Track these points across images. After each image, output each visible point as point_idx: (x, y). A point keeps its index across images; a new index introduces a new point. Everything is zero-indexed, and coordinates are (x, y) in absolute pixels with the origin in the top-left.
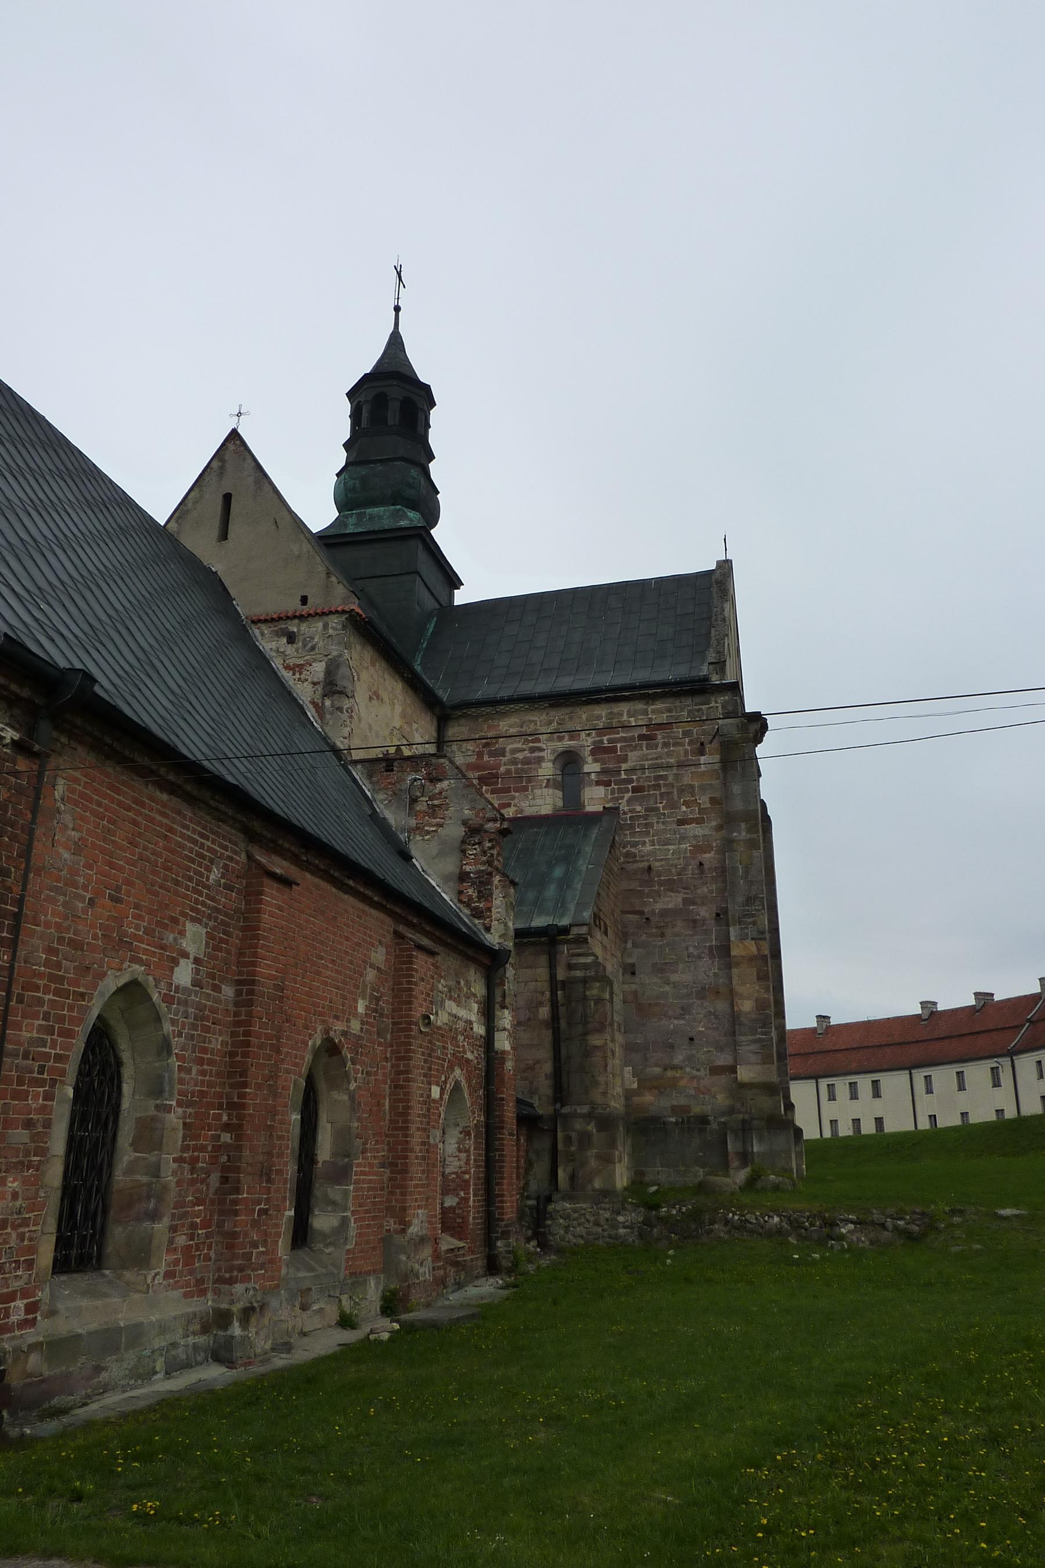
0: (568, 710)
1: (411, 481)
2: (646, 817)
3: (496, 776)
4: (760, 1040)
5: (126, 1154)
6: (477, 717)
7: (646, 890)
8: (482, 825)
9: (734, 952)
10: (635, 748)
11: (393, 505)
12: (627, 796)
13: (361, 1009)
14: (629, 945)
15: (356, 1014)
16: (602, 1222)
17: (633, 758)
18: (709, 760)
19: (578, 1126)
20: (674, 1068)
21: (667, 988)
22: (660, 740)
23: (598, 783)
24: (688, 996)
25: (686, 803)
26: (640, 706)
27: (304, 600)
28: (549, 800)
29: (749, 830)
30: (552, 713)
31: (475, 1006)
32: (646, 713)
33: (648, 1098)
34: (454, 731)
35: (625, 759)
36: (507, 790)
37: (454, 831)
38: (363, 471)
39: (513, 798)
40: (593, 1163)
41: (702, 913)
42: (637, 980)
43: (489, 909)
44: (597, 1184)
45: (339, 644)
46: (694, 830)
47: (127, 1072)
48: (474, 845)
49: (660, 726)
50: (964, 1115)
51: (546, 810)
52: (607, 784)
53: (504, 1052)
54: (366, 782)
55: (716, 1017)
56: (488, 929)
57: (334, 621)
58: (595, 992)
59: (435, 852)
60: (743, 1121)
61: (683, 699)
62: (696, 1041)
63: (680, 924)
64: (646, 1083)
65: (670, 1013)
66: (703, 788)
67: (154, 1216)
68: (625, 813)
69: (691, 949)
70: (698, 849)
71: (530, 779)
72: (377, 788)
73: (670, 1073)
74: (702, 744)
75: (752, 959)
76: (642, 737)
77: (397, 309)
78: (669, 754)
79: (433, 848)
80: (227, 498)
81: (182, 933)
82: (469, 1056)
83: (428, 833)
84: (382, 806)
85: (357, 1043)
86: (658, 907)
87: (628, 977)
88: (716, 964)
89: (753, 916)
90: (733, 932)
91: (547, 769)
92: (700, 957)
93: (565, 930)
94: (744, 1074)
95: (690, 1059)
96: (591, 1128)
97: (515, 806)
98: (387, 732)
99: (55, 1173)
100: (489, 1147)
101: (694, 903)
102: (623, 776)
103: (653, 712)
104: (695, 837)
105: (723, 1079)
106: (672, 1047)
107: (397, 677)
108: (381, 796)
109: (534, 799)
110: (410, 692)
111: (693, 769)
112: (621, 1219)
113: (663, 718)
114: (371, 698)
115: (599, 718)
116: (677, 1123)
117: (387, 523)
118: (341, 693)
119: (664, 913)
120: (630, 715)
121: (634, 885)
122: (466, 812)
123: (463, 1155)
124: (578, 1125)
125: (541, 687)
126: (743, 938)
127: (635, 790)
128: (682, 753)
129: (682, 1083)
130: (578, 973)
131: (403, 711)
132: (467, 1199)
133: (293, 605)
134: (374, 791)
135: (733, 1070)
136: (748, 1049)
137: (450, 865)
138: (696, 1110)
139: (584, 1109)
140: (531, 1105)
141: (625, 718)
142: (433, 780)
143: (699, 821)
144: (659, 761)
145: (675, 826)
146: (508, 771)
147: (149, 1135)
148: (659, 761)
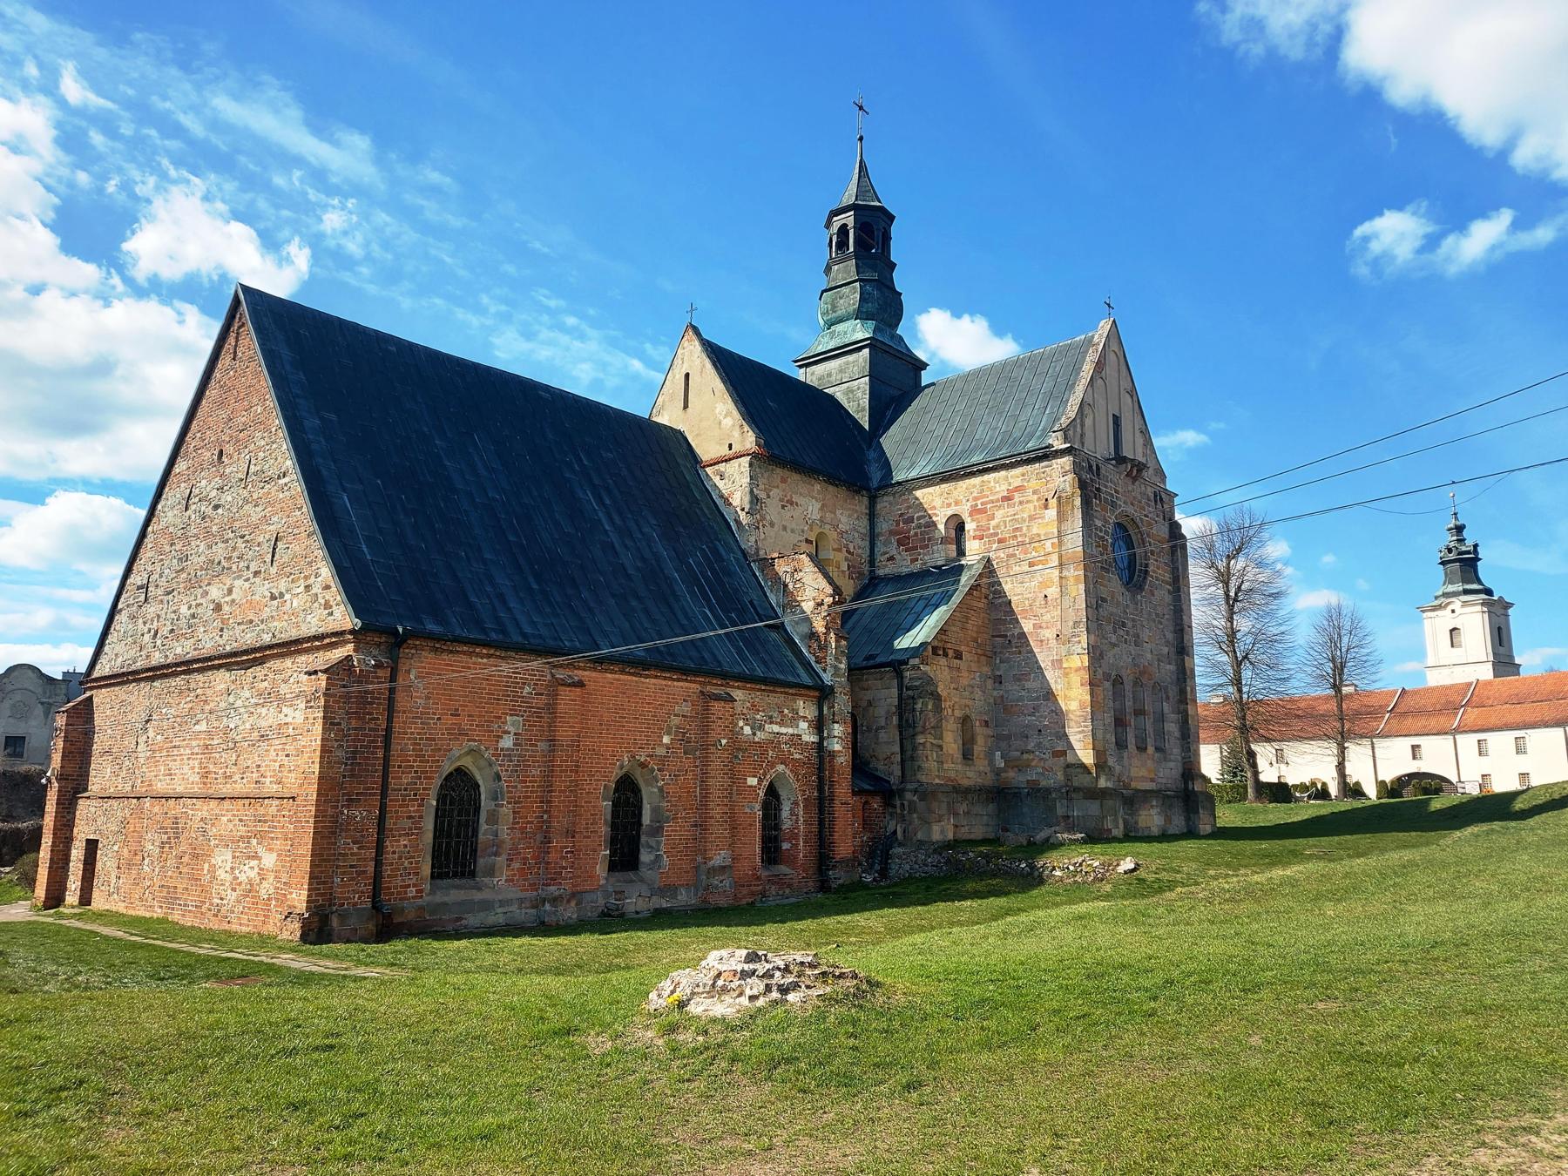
5: (483, 827)
13: (666, 740)
15: (661, 744)
17: (999, 514)
18: (1052, 513)
22: (1017, 500)
24: (1038, 698)
27: (730, 446)
33: (1011, 774)
44: (920, 836)
47: (482, 789)
49: (1018, 489)
50: (1524, 776)
67: (496, 854)
70: (1044, 584)
76: (1005, 499)
77: (861, 139)
80: (687, 375)
81: (505, 723)
82: (797, 756)
85: (663, 759)
99: (429, 837)
100: (821, 812)
110: (831, 488)
124: (908, 796)
127: (1000, 541)
133: (725, 451)
138: (1044, 783)
139: (915, 785)
147: (493, 818)
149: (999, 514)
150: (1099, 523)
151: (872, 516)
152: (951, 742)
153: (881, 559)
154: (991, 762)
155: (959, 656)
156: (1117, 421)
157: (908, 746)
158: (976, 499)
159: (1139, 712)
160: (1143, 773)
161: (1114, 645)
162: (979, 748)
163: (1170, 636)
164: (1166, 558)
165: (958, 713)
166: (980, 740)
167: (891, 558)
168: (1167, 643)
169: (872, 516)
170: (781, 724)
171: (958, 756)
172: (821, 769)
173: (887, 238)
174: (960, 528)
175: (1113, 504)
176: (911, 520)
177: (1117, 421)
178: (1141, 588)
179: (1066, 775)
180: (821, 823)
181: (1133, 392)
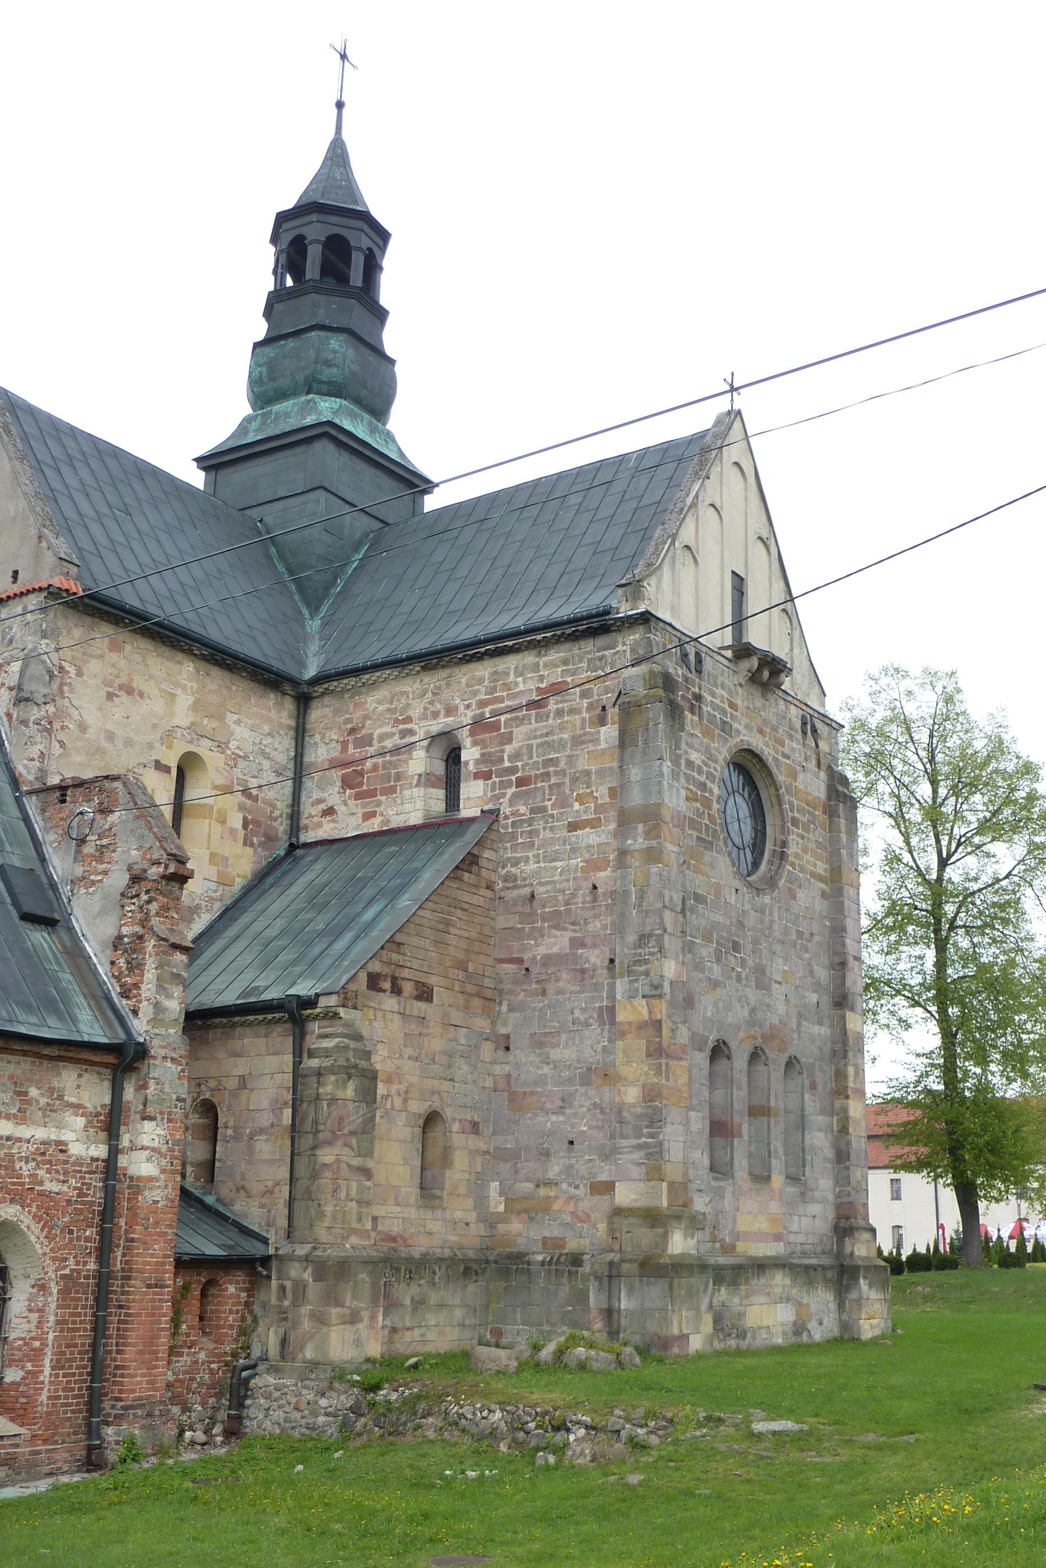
0: (444, 673)
1: (330, 356)
2: (530, 822)
3: (361, 774)
4: (645, 1146)
6: (343, 691)
7: (527, 927)
8: (145, 871)
9: (620, 1017)
10: (521, 721)
11: (308, 393)
12: (511, 791)
14: (504, 1008)
16: (303, 1405)
17: (519, 732)
18: (609, 733)
19: (293, 1273)
20: (548, 1183)
21: (546, 1070)
23: (477, 776)
24: (571, 1080)
25: (580, 799)
26: (528, 658)
28: (420, 804)
29: (648, 835)
30: (427, 679)
31: (80, 1122)
32: (536, 667)
33: (516, 1226)
34: (319, 713)
35: (508, 739)
36: (372, 793)
37: (119, 879)
38: (270, 351)
39: (379, 804)
40: (306, 1325)
41: (593, 960)
42: (511, 1058)
43: (136, 986)
44: (309, 1353)
45: (35, 633)
46: (588, 837)
48: (132, 898)
51: (415, 818)
52: (487, 776)
53: (140, 1179)
54: (39, 818)
55: (602, 1112)
56: (135, 1012)
57: (33, 601)
58: (329, 1089)
59: (96, 909)
60: (611, 1264)
61: (582, 643)
62: (576, 1145)
63: (565, 976)
64: (517, 1205)
65: (548, 1106)
66: (601, 773)
68: (506, 818)
69: (577, 1013)
70: (592, 866)
71: (398, 777)
72: (49, 825)
73: (542, 1192)
74: (604, 708)
75: (641, 1026)
76: (532, 705)
77: (340, 105)
78: (562, 728)
79: (95, 903)
82: (55, 1187)
83: (93, 883)
84: (51, 850)
86: (541, 951)
87: (501, 1053)
88: (606, 1034)
89: (646, 962)
90: (621, 986)
91: (419, 762)
92: (587, 1025)
93: (310, 1002)
94: (625, 1195)
95: (568, 1169)
96: (307, 1276)
97: (381, 815)
98: (155, 737)
101: (583, 945)
102: (507, 764)
103: (546, 666)
104: (589, 847)
105: (602, 1203)
106: (547, 1154)
107: (180, 656)
108: (51, 837)
109: (402, 804)
110: (216, 672)
111: (591, 747)
112: (323, 1402)
113: (555, 675)
114: (110, 696)
115: (481, 681)
116: (543, 1263)
117: (293, 423)
118: (27, 700)
119: (548, 960)
120: (518, 674)
121: (514, 921)
122: (134, 853)
123: (34, 1316)
124: (294, 1271)
125: (424, 643)
126: (632, 996)
127: (521, 782)
128: (578, 724)
129: (556, 1206)
130: (314, 1063)
131: (197, 702)
132: (35, 1374)
134: (46, 830)
135: (609, 1187)
136: (630, 1159)
137: (108, 928)
138: (572, 1245)
140: (265, 1241)
141: (512, 678)
142: (104, 811)
143: (593, 824)
144: (550, 738)
145: (564, 833)
146: (375, 767)
148: (550, 738)
149: (519, 732)
150: (695, 756)
151: (300, 733)
152: (395, 1157)
153: (310, 810)
154: (481, 1201)
155: (425, 994)
156: (739, 583)
157: (301, 1169)
158: (482, 704)
159: (758, 1111)
160: (762, 1224)
161: (715, 984)
162: (459, 1170)
163: (823, 974)
164: (818, 835)
165: (418, 1107)
166: (460, 1160)
167: (330, 811)
168: (817, 987)
169: (300, 733)
170: (21, 1117)
171: (410, 1190)
172: (108, 1213)
173: (372, 267)
174: (453, 757)
175: (726, 728)
176: (367, 741)
177: (739, 583)
178: (771, 882)
179: (612, 1232)
180: (99, 1327)
181: (768, 541)
